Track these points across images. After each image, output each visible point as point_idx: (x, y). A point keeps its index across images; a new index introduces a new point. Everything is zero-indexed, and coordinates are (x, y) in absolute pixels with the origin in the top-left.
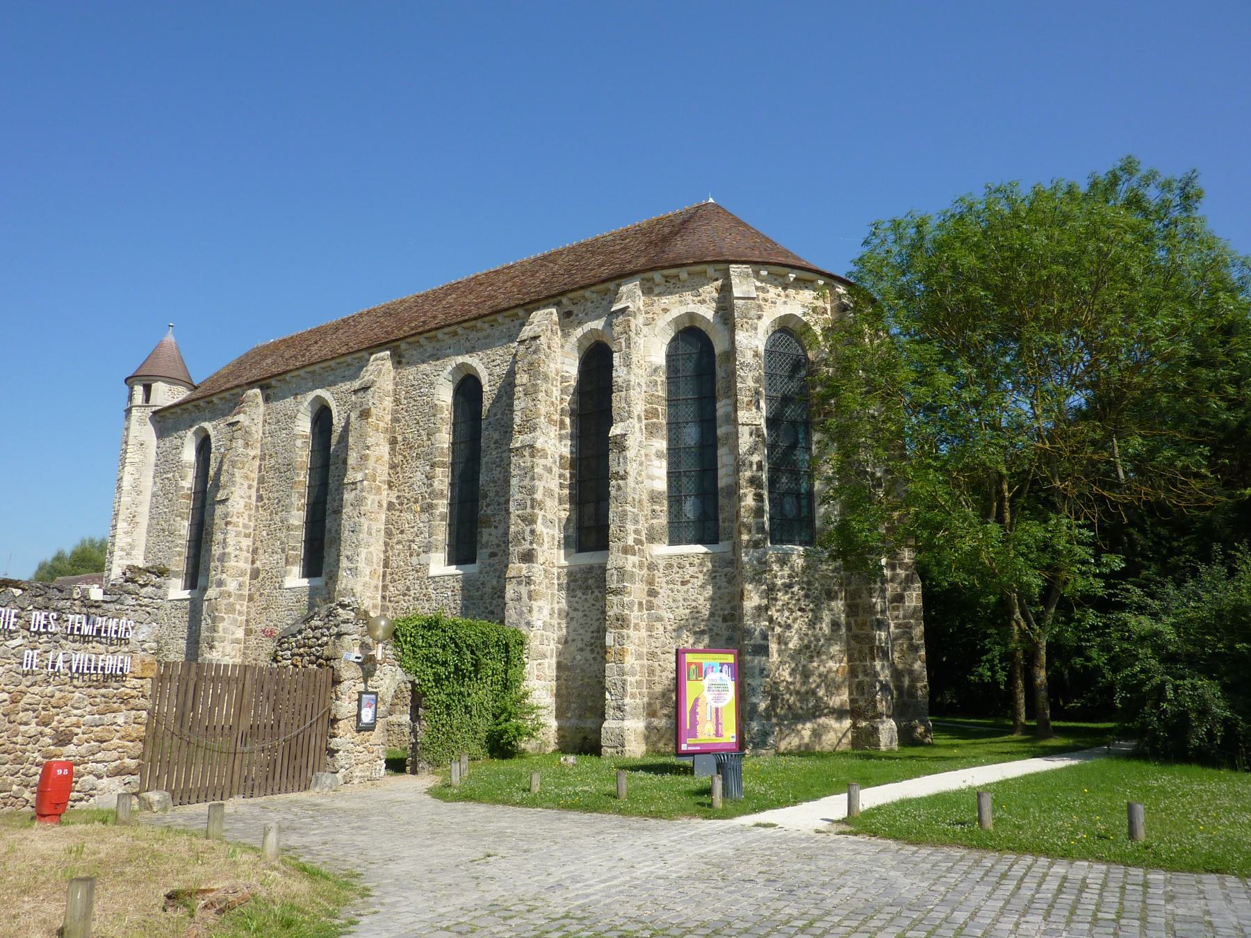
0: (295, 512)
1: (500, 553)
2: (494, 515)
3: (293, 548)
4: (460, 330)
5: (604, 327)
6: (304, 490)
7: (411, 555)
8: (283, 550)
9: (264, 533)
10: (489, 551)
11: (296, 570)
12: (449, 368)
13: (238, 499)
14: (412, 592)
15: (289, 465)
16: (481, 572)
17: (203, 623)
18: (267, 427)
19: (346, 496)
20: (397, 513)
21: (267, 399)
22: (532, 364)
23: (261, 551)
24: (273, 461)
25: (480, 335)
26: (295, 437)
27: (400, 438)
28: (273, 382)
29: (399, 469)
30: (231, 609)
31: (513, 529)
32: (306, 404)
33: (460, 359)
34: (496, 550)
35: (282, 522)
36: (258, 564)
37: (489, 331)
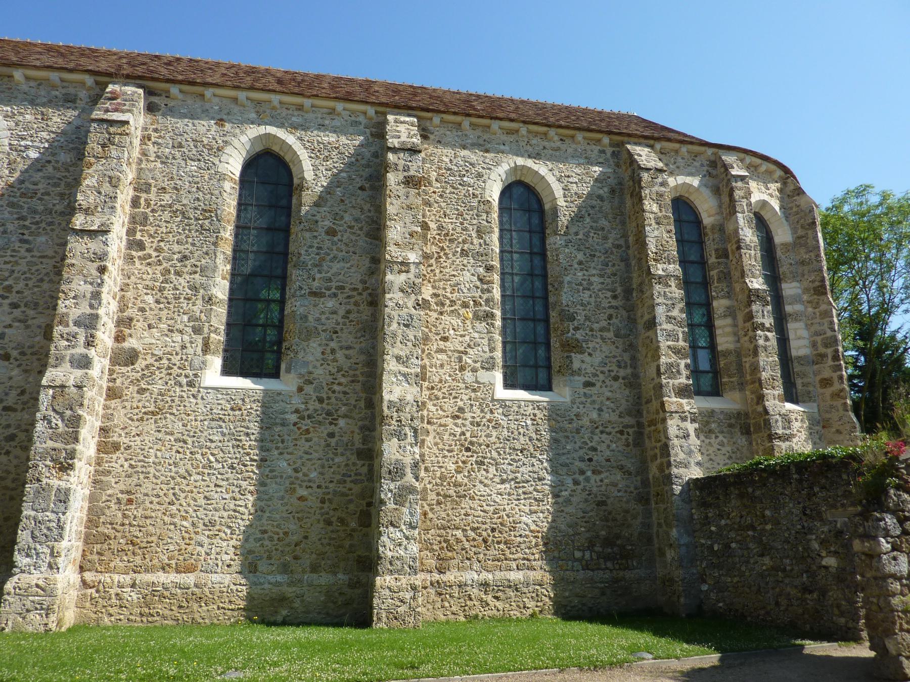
0: (218, 279)
1: (598, 384)
2: (587, 341)
3: (216, 331)
4: (523, 130)
5: (699, 186)
6: (229, 252)
7: (462, 369)
8: (197, 331)
9: (150, 299)
10: (582, 379)
11: (216, 362)
12: (505, 167)
13: (115, 236)
14: (468, 415)
15: (211, 213)
16: (573, 402)
17: (40, 427)
18: (152, 149)
19: (389, 277)
20: (435, 315)
21: (151, 108)
22: (661, 196)
23: (140, 325)
24: (167, 198)
25: (546, 144)
26: (222, 177)
27: (433, 225)
28: (174, 90)
29: (433, 261)
30: (91, 411)
31: (663, 360)
32: (244, 139)
33: (520, 161)
34: (593, 380)
35: (194, 288)
36: (131, 343)
37: (559, 144)
